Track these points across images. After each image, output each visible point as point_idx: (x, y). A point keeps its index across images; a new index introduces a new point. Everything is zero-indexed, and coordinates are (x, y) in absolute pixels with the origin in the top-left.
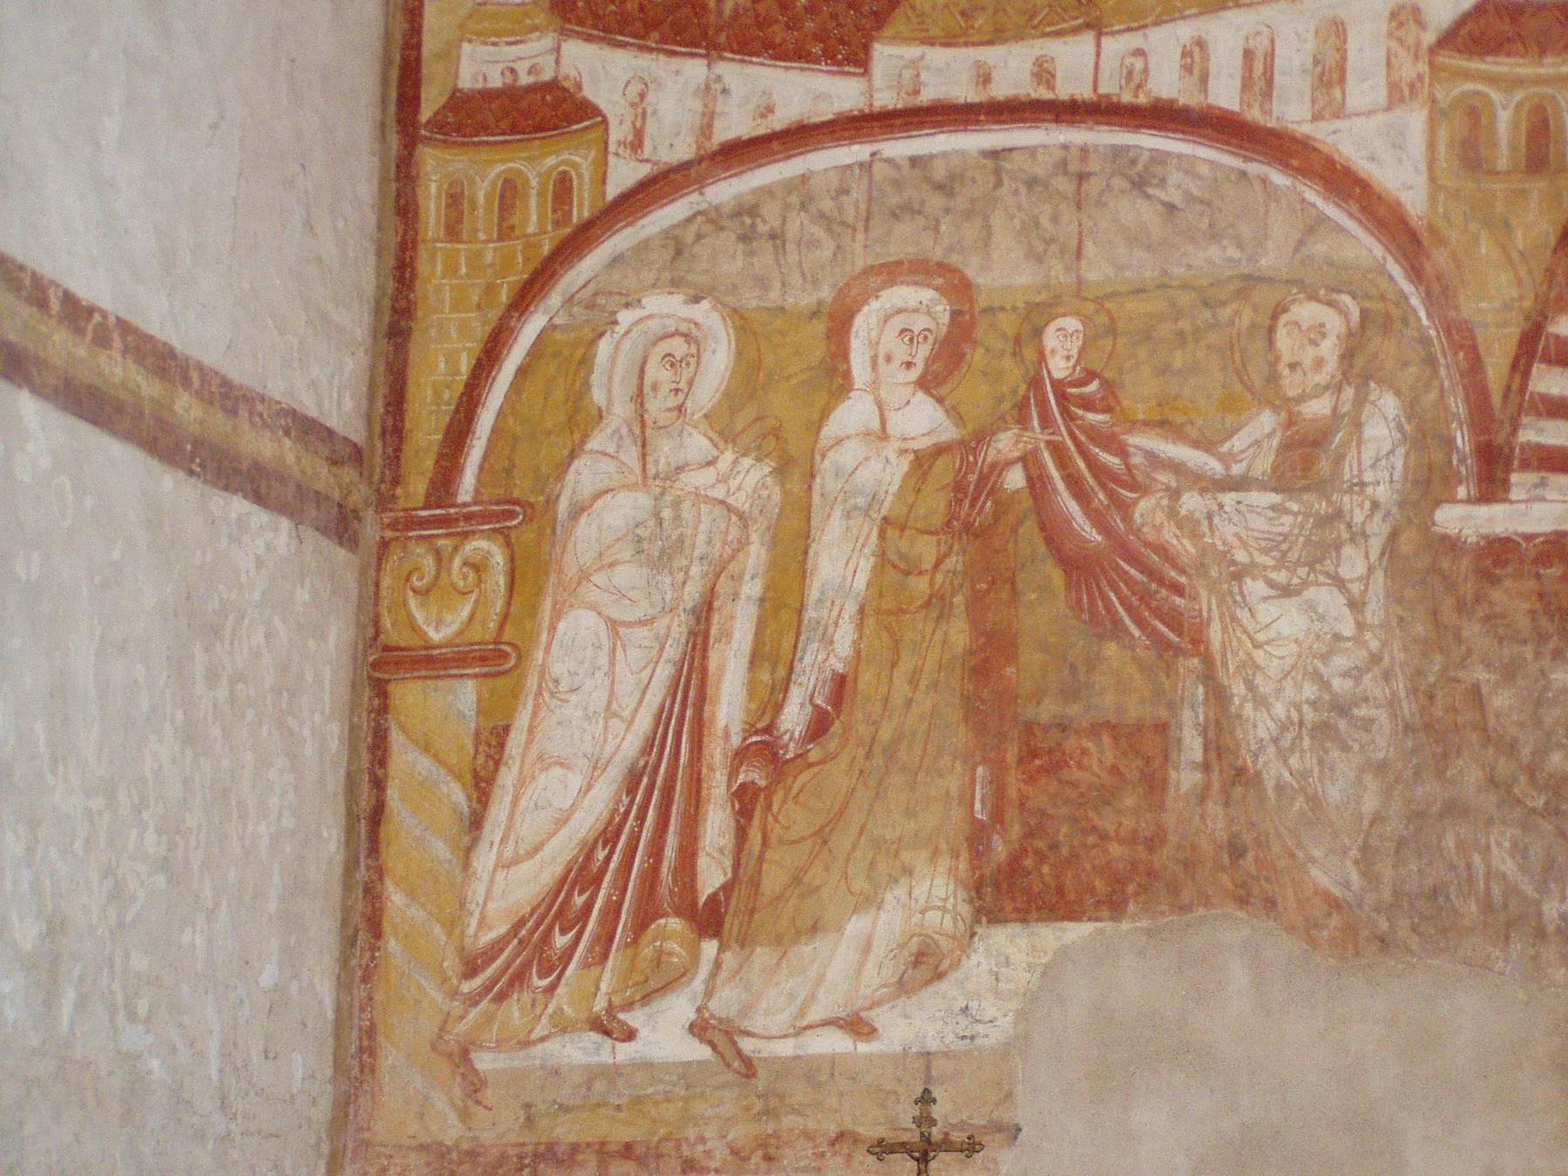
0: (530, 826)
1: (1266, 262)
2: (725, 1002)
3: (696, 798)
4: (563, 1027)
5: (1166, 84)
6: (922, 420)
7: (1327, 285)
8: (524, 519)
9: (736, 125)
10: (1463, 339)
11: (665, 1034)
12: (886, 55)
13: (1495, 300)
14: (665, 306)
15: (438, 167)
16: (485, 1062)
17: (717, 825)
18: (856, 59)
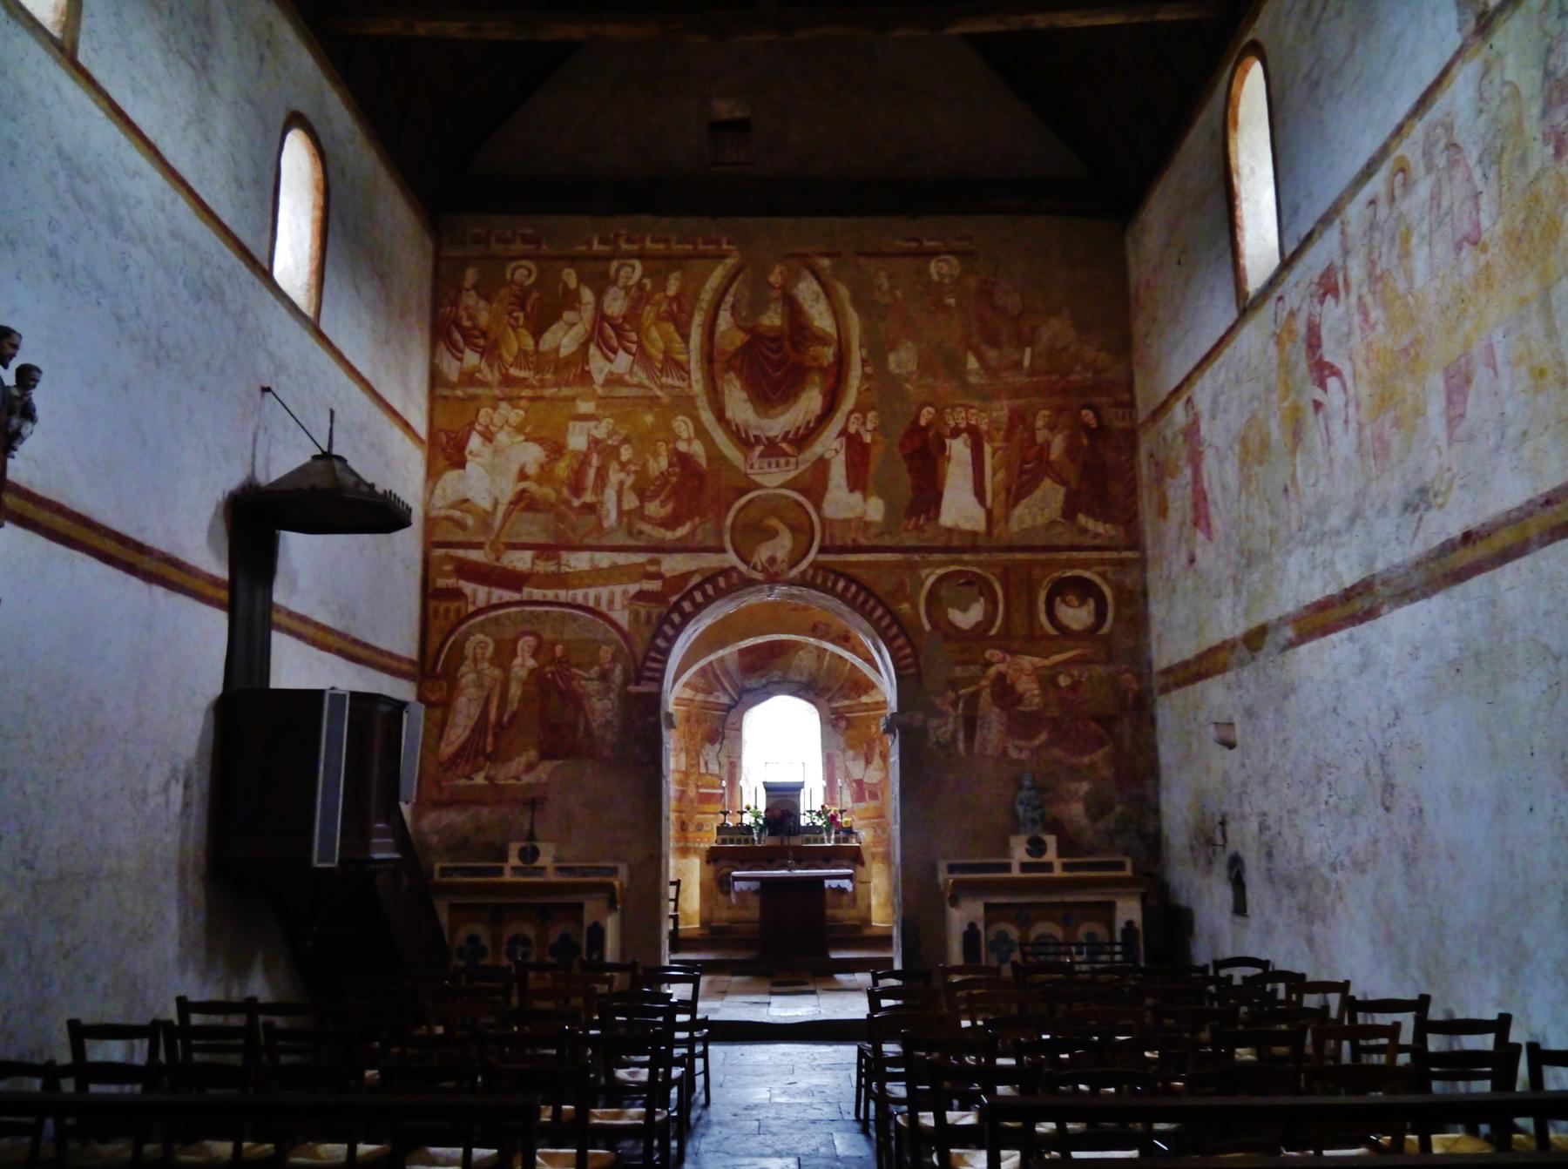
0: (453, 737)
1: (599, 637)
2: (492, 772)
3: (486, 736)
4: (458, 777)
5: (580, 600)
6: (531, 663)
7: (608, 642)
8: (451, 677)
9: (494, 600)
10: (633, 654)
11: (480, 779)
12: (526, 590)
13: (640, 647)
14: (480, 637)
15: (432, 604)
16: (444, 784)
17: (490, 740)
18: (519, 589)
